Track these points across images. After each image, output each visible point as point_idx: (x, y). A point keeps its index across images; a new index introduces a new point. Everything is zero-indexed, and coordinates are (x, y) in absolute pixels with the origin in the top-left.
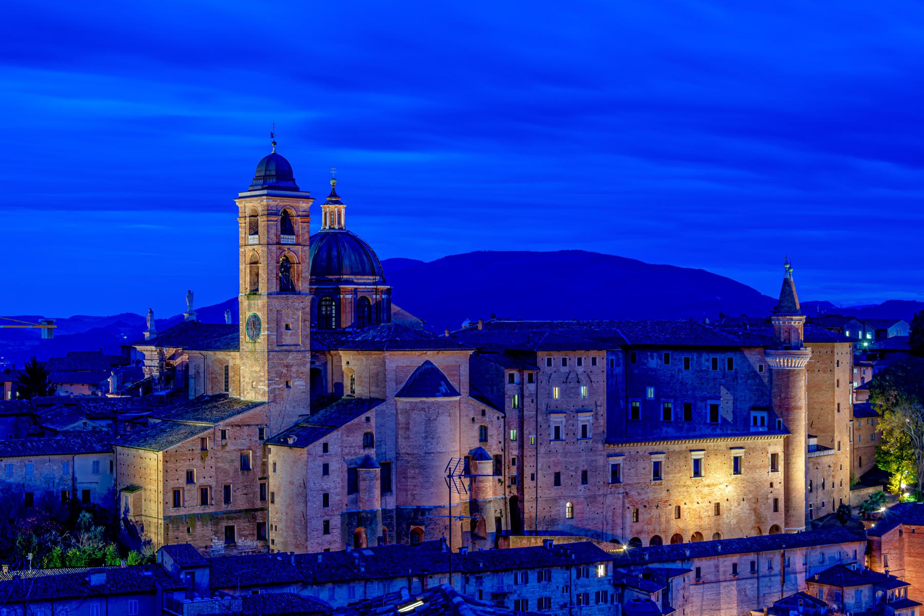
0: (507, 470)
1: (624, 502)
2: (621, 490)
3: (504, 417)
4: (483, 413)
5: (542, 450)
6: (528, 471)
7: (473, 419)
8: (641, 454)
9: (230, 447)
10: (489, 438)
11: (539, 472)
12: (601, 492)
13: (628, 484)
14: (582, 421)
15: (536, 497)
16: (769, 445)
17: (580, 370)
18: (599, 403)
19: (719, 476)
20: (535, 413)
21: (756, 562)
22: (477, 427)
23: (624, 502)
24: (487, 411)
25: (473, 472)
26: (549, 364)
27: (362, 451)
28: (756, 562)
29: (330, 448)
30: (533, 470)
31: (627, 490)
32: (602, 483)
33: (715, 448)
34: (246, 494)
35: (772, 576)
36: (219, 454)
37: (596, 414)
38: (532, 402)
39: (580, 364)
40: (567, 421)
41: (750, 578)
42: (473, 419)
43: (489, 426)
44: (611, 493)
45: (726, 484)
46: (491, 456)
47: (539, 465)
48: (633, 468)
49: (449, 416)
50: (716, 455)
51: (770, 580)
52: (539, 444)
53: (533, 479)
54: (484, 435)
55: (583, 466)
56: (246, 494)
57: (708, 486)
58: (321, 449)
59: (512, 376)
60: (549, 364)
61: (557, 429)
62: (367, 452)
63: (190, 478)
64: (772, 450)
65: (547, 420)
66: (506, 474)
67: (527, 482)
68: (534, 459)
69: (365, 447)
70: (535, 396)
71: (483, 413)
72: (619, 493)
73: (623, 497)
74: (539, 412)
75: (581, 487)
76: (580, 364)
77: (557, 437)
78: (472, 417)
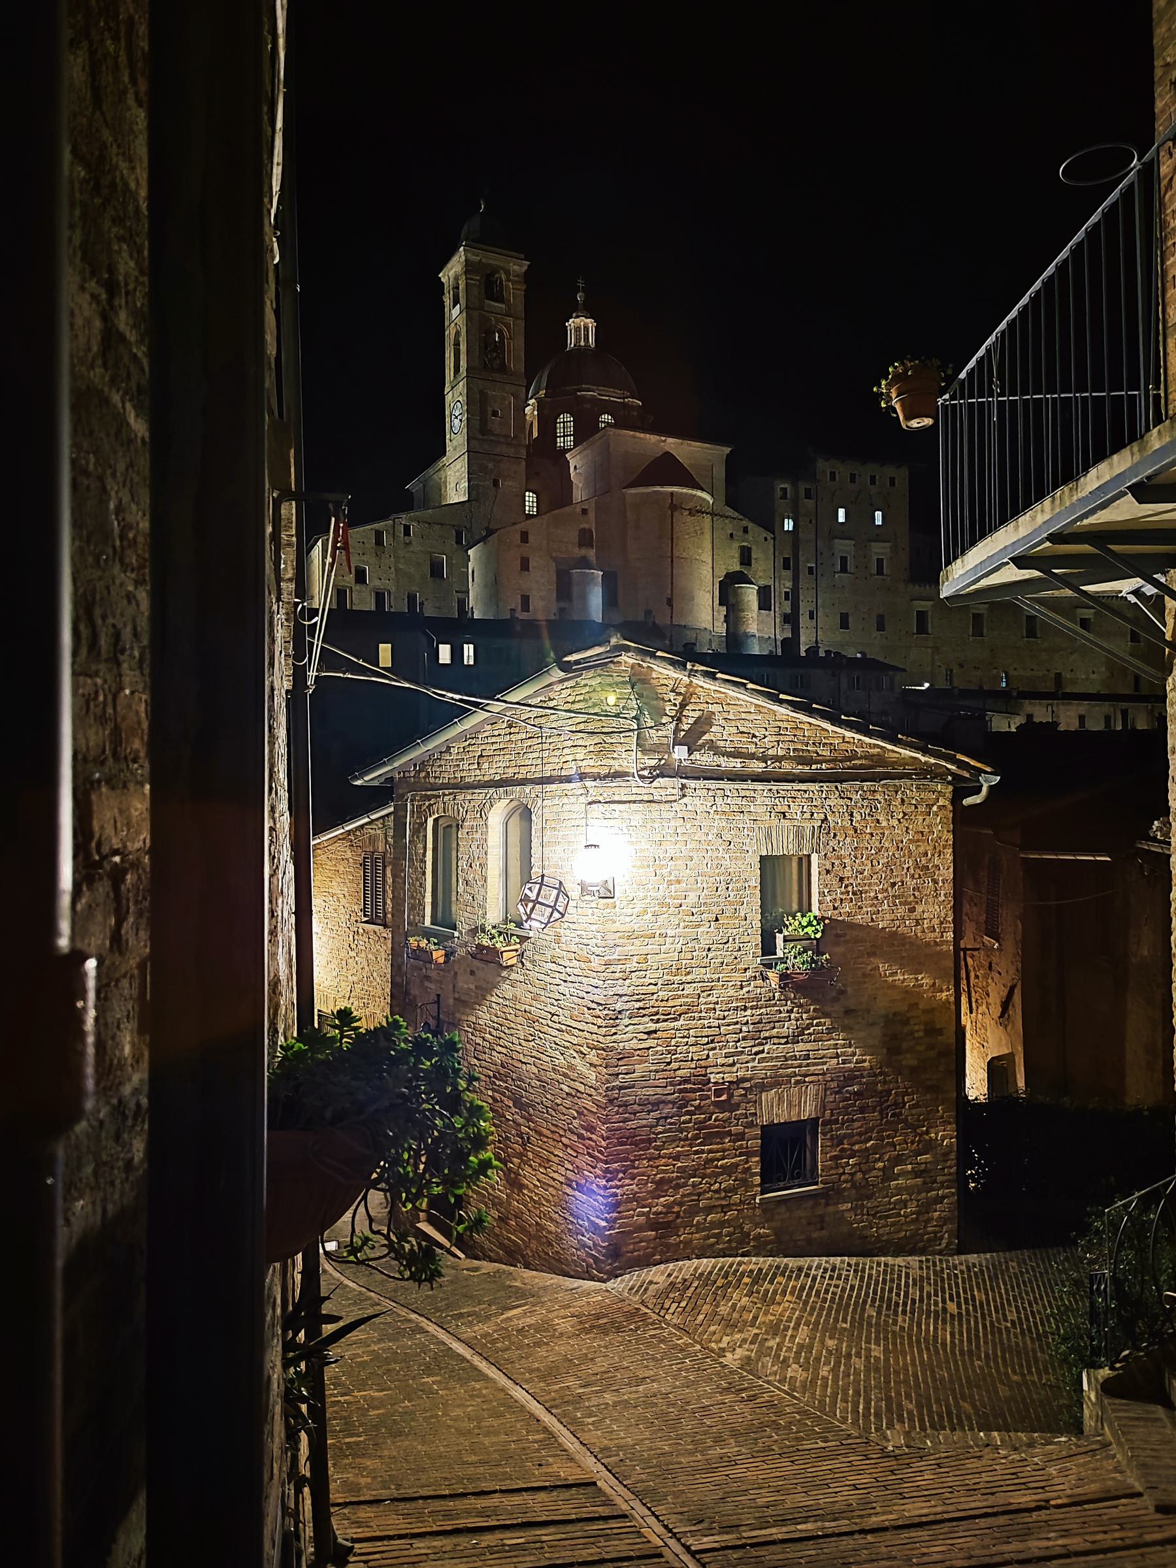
1: (933, 659)
6: (804, 609)
7: (731, 535)
9: (416, 547)
10: (753, 561)
11: (820, 609)
17: (874, 490)
22: (736, 545)
23: (933, 659)
25: (732, 600)
26: (833, 477)
27: (576, 550)
29: (531, 538)
34: (439, 608)
36: (401, 553)
42: (731, 535)
43: (754, 547)
52: (819, 576)
53: (811, 617)
54: (746, 557)
56: (439, 608)
58: (518, 537)
59: (784, 490)
60: (833, 477)
62: (583, 552)
63: (360, 577)
67: (804, 620)
69: (581, 545)
71: (746, 530)
77: (844, 569)
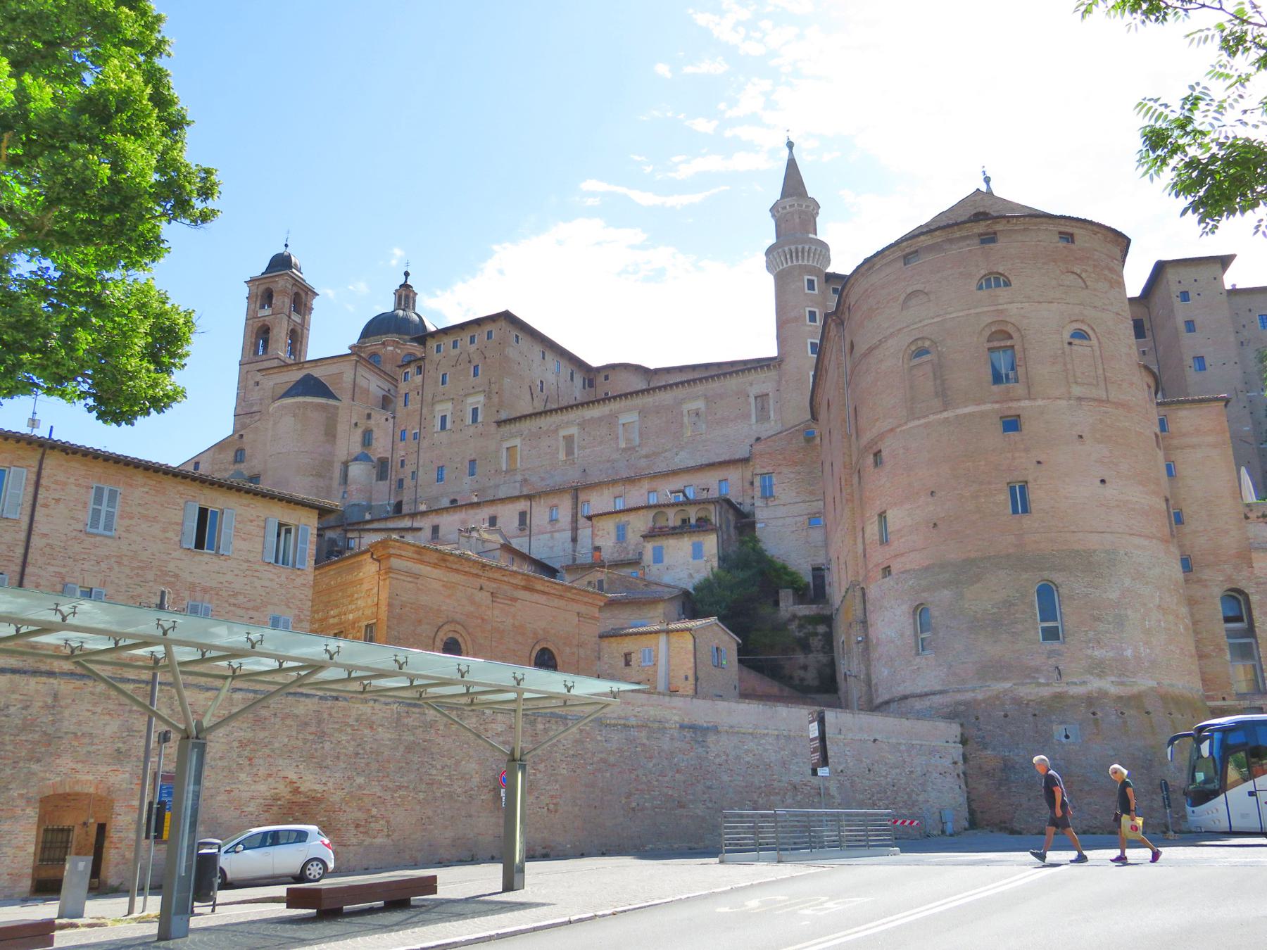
0: (394, 473)
2: (519, 478)
3: (394, 418)
4: (369, 416)
5: (424, 444)
7: (356, 424)
8: (545, 429)
10: (374, 441)
11: (421, 469)
12: (492, 483)
13: (528, 469)
14: (471, 404)
15: (416, 498)
16: (751, 384)
17: (473, 348)
18: (493, 380)
19: (663, 441)
20: (420, 406)
21: (529, 512)
22: (359, 431)
24: (373, 413)
26: (438, 350)
27: (232, 467)
28: (529, 512)
30: (414, 468)
31: (527, 476)
32: (493, 472)
33: (657, 404)
35: (555, 531)
37: (490, 392)
38: (418, 393)
39: (472, 341)
40: (454, 407)
41: (518, 537)
43: (375, 429)
44: (505, 482)
45: (675, 450)
46: (374, 459)
47: (421, 462)
48: (535, 448)
49: (294, 416)
50: (658, 413)
51: (552, 537)
52: (422, 439)
55: (471, 455)
57: (646, 456)
61: (444, 419)
64: (754, 391)
65: (432, 411)
66: (393, 477)
67: (408, 482)
68: (415, 455)
70: (421, 388)
72: (515, 482)
73: (521, 486)
74: (424, 403)
75: (467, 479)
76: (472, 341)
77: (443, 427)
78: (355, 422)
